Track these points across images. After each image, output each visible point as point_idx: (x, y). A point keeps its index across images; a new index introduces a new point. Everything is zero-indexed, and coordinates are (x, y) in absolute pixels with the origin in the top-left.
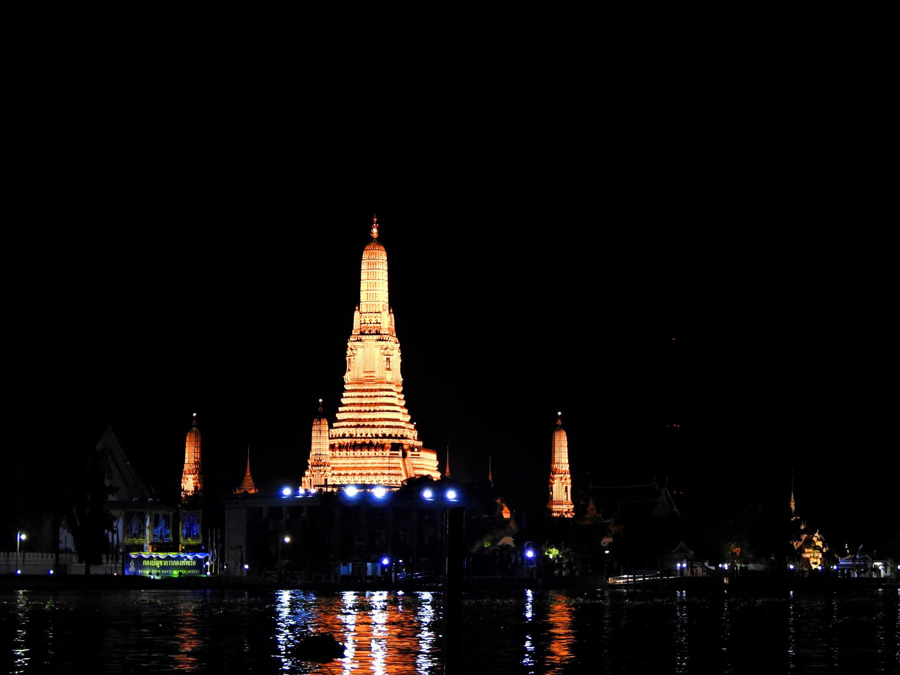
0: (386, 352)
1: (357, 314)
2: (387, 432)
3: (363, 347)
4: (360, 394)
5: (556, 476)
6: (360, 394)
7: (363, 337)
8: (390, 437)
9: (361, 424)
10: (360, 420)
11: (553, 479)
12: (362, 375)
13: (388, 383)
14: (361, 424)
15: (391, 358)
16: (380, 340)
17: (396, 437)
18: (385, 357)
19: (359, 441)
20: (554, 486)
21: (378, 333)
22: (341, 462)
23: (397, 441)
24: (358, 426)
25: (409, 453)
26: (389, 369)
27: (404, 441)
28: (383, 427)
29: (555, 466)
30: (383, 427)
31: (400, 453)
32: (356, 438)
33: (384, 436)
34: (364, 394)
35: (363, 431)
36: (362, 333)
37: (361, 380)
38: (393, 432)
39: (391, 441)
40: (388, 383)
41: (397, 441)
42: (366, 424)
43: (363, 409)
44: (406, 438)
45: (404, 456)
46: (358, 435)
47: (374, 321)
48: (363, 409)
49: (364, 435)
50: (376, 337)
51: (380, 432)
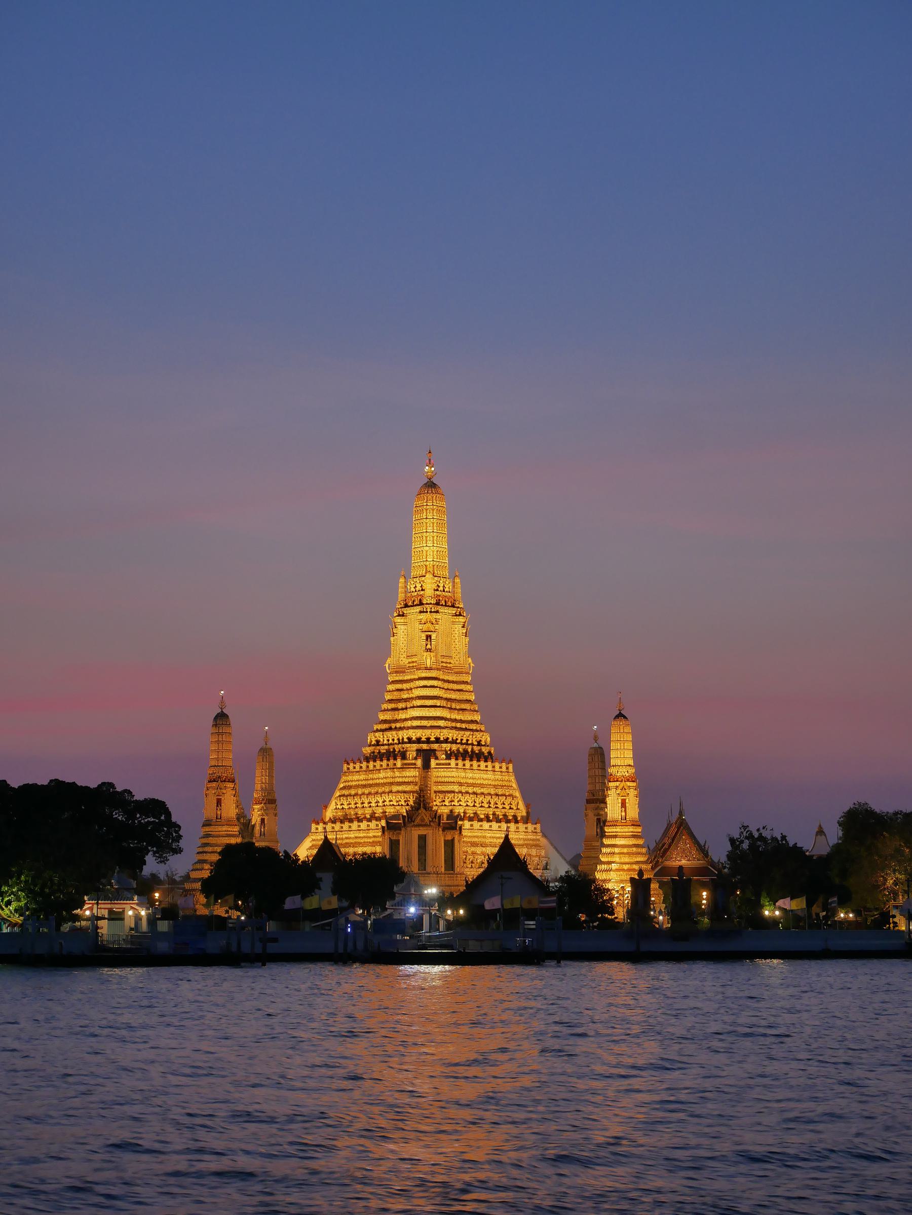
0: (425, 627)
1: (402, 580)
2: (414, 734)
3: (405, 624)
4: (399, 686)
5: (611, 784)
6: (399, 686)
7: (406, 611)
8: (419, 741)
9: (393, 726)
10: (396, 721)
11: (608, 789)
12: (405, 661)
13: (426, 669)
14: (393, 726)
15: (434, 636)
16: (421, 612)
17: (428, 741)
18: (424, 636)
19: (383, 749)
20: (609, 800)
21: (421, 604)
22: (356, 777)
23: (425, 746)
24: (390, 729)
25: (433, 763)
26: (430, 650)
27: (435, 746)
28: (408, 728)
29: (612, 770)
30: (408, 728)
31: (419, 762)
32: (383, 745)
33: (410, 741)
34: (405, 686)
35: (389, 734)
36: (406, 606)
37: (399, 667)
38: (424, 734)
39: (415, 746)
40: (426, 669)
41: (425, 746)
42: (398, 725)
43: (401, 705)
44: (446, 741)
45: (426, 766)
46: (385, 742)
47: (419, 588)
48: (401, 705)
49: (391, 741)
50: (418, 609)
51: (404, 735)
